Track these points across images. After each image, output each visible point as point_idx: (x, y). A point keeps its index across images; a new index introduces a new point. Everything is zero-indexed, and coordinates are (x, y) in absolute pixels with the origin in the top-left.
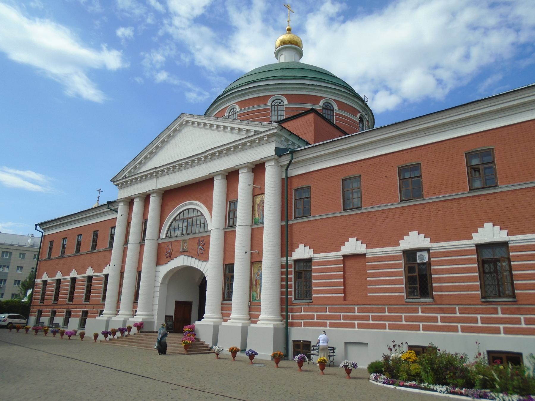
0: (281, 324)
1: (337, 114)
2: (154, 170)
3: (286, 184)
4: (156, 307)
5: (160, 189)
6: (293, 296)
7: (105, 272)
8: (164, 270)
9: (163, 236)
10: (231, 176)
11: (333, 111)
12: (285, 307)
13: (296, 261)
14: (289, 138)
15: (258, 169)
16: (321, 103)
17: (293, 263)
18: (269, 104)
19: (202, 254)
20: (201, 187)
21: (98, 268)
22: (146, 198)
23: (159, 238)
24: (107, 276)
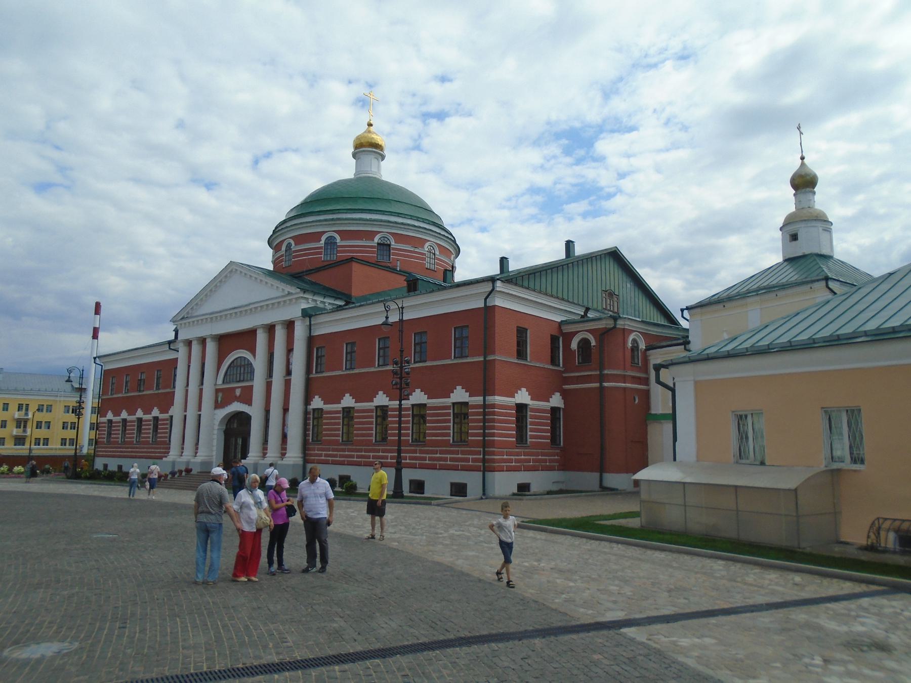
0: (300, 461)
1: (394, 249)
3: (311, 341)
4: (215, 448)
7: (170, 413)
8: (223, 413)
9: (220, 381)
11: (389, 245)
12: (305, 446)
13: (314, 410)
14: (315, 298)
15: (290, 325)
16: (376, 240)
18: (323, 242)
19: (248, 401)
20: (246, 338)
21: (164, 410)
22: (203, 341)
23: (216, 385)
24: (172, 417)
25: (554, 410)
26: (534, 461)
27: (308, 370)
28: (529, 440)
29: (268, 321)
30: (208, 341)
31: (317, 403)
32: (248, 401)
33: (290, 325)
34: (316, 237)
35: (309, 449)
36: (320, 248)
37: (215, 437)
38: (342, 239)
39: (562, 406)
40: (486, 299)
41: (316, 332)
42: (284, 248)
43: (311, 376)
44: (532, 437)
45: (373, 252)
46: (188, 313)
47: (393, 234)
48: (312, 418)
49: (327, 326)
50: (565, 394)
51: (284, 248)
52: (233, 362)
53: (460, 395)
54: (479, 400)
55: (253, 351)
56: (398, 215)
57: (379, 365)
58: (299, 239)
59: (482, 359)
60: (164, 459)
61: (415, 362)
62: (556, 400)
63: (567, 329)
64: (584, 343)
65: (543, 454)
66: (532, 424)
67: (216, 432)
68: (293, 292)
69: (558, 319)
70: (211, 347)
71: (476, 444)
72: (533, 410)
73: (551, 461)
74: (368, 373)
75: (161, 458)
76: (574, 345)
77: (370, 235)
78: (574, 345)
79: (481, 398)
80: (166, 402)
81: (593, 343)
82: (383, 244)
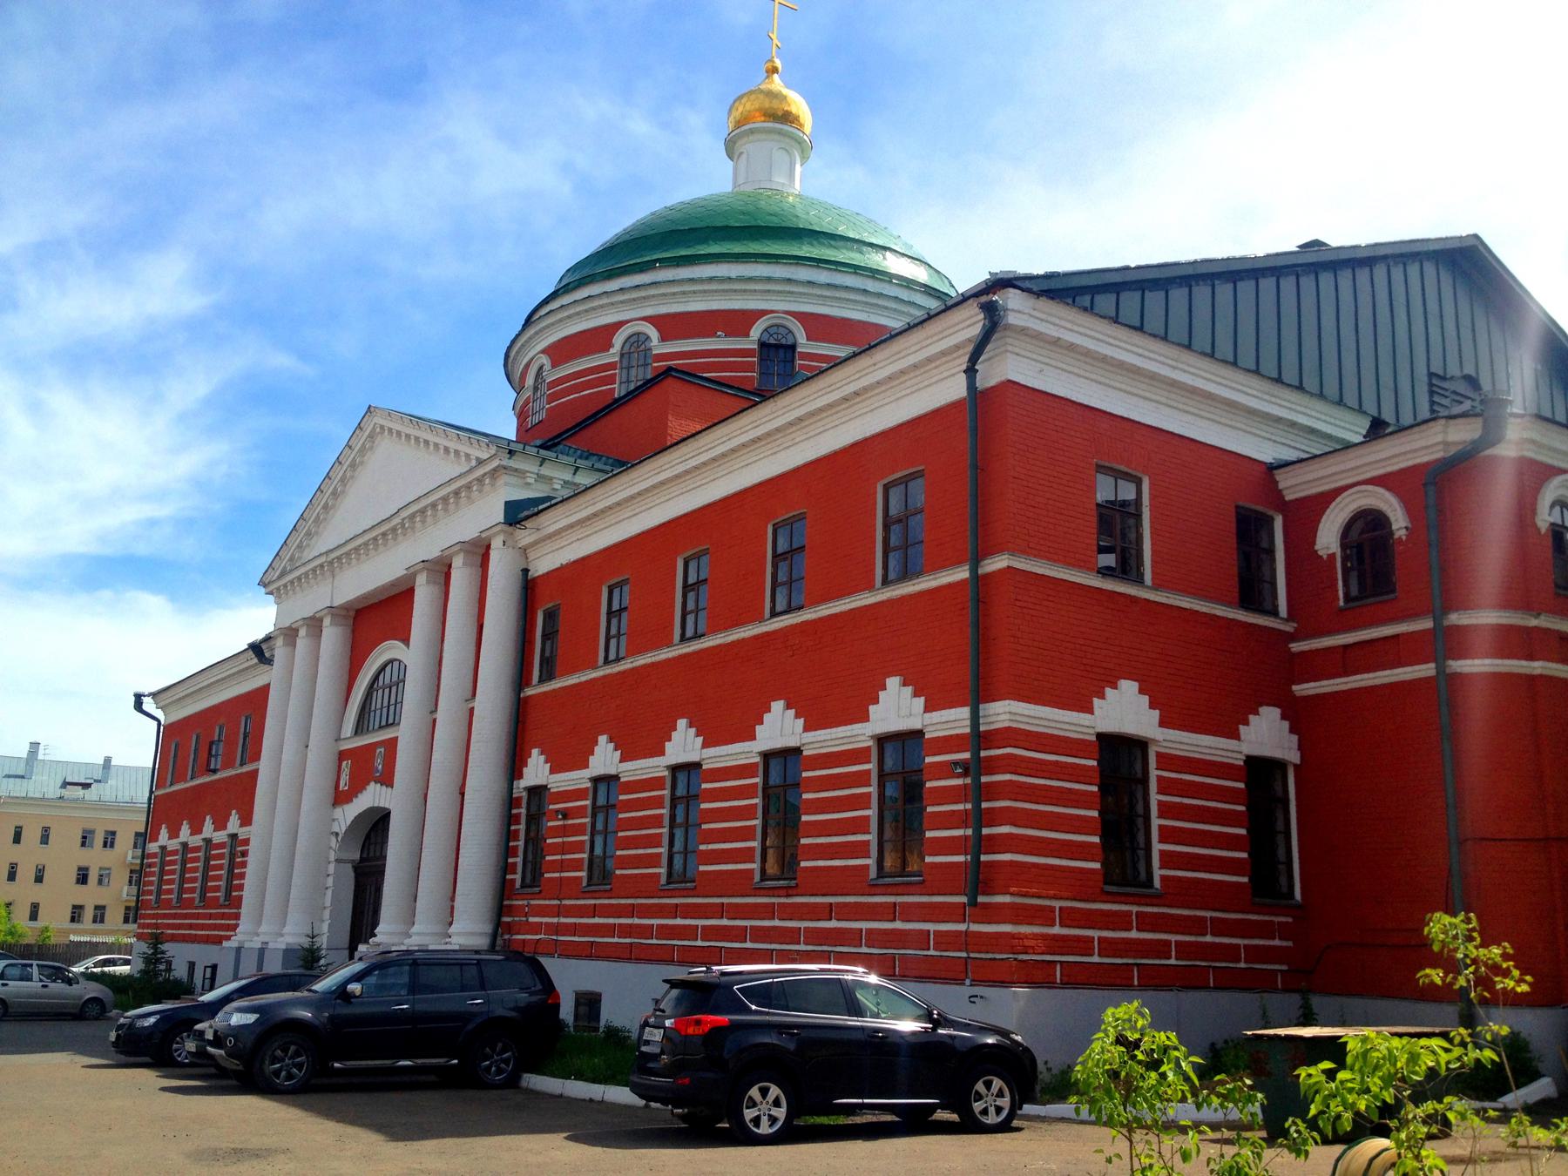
2: (323, 559)
5: (346, 607)
6: (518, 877)
10: (442, 570)
11: (793, 347)
14: (546, 471)
17: (524, 794)
22: (315, 624)
25: (1261, 770)
26: (1183, 950)
27: (522, 677)
28: (1158, 873)
29: (433, 552)
30: (327, 622)
31: (537, 770)
32: (387, 780)
33: (480, 552)
34: (599, 338)
35: (511, 910)
36: (612, 366)
37: (330, 881)
38: (664, 338)
39: (1293, 756)
40: (971, 371)
41: (543, 564)
42: (530, 381)
43: (529, 692)
44: (1168, 860)
45: (748, 367)
46: (291, 559)
47: (802, 317)
48: (525, 817)
49: (563, 544)
50: (1298, 715)
51: (530, 381)
52: (376, 678)
53: (897, 708)
54: (954, 720)
55: (406, 640)
56: (818, 262)
57: (683, 639)
58: (562, 351)
59: (962, 574)
60: (225, 944)
61: (774, 614)
62: (1267, 734)
63: (1294, 486)
64: (1367, 531)
65: (1220, 928)
66: (1165, 810)
67: (331, 868)
68: (485, 456)
69: (1265, 452)
70: (333, 638)
71: (943, 879)
72: (1166, 761)
73: (1254, 954)
74: (653, 664)
75: (218, 941)
76: (1328, 538)
77: (738, 322)
78: (1328, 538)
79: (964, 713)
80: (241, 796)
81: (1399, 523)
82: (778, 347)
